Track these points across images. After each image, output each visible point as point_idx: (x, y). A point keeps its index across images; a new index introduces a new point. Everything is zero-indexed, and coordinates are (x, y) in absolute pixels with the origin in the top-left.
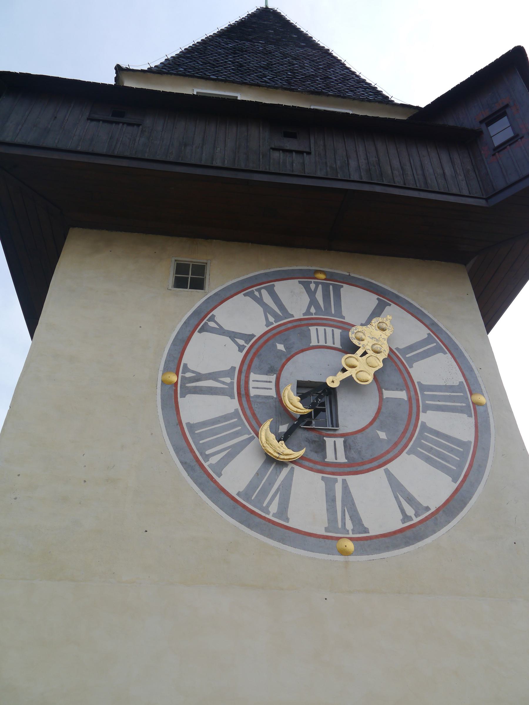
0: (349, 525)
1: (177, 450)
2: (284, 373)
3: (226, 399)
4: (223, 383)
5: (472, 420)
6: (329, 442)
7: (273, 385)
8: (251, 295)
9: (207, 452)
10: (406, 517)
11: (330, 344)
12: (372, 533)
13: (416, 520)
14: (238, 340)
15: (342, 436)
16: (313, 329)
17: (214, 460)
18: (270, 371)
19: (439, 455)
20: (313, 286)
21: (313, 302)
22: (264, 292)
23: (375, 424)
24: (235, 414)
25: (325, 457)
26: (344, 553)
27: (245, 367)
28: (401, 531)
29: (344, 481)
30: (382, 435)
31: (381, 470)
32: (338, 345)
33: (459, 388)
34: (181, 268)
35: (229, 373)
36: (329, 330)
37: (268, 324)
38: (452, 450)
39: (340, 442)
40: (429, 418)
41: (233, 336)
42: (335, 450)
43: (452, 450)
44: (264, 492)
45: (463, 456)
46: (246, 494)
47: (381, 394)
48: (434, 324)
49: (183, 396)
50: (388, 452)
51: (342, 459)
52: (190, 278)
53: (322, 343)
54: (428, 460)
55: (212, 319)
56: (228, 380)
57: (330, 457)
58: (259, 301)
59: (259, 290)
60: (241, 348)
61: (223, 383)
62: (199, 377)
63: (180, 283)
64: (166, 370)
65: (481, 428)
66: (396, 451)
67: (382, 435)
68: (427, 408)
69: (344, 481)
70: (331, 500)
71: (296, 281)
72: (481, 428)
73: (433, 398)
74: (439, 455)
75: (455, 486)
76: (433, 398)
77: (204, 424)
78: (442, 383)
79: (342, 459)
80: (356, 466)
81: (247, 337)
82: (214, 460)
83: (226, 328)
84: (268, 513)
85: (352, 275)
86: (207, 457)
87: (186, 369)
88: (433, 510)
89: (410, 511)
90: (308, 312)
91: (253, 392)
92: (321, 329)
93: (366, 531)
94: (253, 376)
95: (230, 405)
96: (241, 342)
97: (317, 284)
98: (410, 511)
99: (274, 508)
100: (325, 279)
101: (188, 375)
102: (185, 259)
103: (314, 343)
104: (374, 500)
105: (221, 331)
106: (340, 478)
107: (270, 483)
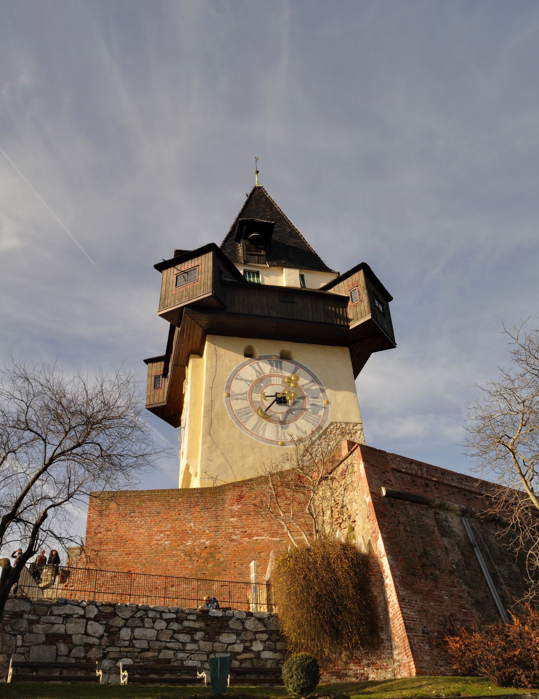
3: (245, 401)
20: (272, 362)
24: (249, 407)
32: (280, 383)
35: (246, 393)
36: (278, 378)
37: (257, 376)
41: (246, 381)
44: (258, 428)
46: (253, 429)
53: (275, 383)
60: (249, 385)
82: (243, 420)
86: (241, 419)
90: (270, 372)
91: (253, 400)
92: (275, 378)
95: (246, 403)
96: (249, 383)
99: (261, 433)
105: (242, 379)
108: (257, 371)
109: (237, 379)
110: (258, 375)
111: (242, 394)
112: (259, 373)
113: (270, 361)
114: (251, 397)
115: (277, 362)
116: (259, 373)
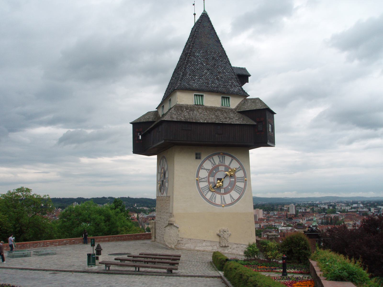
0: (224, 203)
1: (199, 192)
2: (215, 177)
4: (205, 180)
5: (244, 184)
6: (222, 189)
7: (213, 179)
8: (209, 160)
9: (204, 192)
10: (232, 201)
11: (222, 170)
12: (227, 204)
13: (233, 202)
14: (207, 171)
15: (223, 188)
16: (220, 167)
17: (205, 194)
18: (212, 177)
19: (238, 190)
20: (220, 156)
21: (220, 161)
22: (211, 159)
23: (228, 186)
25: (221, 192)
26: (223, 207)
27: (209, 176)
28: (231, 203)
29: (223, 196)
30: (230, 187)
31: (229, 194)
32: (224, 170)
33: (243, 177)
34: (196, 154)
35: (206, 177)
36: (222, 167)
38: (240, 189)
39: (223, 189)
40: (238, 184)
42: (222, 191)
43: (240, 189)
44: (212, 198)
45: (241, 190)
46: (210, 199)
47: (230, 180)
48: (241, 163)
49: (199, 183)
50: (230, 190)
51: (223, 192)
52: (198, 157)
53: (221, 170)
54: (236, 192)
55: (203, 166)
56: (206, 179)
57: (222, 192)
58: (211, 161)
59: (210, 159)
60: (208, 172)
61: (205, 180)
62: (202, 179)
63: (197, 158)
64: (196, 178)
65: (245, 185)
66: (231, 190)
67: (230, 187)
68: (237, 182)
69: (223, 196)
70: (221, 199)
71: (217, 156)
72: (245, 185)
73: (239, 180)
74: (238, 190)
75: (239, 196)
76: (239, 180)
77: (203, 188)
78: (240, 177)
79: (223, 192)
80: (225, 193)
81: (209, 170)
82: (205, 194)
83: (206, 168)
84: (213, 201)
85: (227, 153)
86: (204, 193)
87: (200, 177)
88: (236, 200)
89: (232, 200)
90: (219, 163)
91: (210, 181)
92: (221, 167)
93: (226, 203)
94: (210, 178)
95: (206, 184)
96: (208, 171)
97: (221, 156)
98: (232, 200)
99: (214, 201)
100: (222, 155)
101: (200, 178)
102: (197, 152)
103: (220, 170)
104: (227, 198)
105: (204, 169)
106: (223, 195)
107: (213, 197)
108: (212, 163)
109: (202, 169)
110: (213, 165)
111: (204, 178)
112: (213, 164)
113: (219, 156)
114: (209, 179)
115: (222, 156)
116: (213, 164)
